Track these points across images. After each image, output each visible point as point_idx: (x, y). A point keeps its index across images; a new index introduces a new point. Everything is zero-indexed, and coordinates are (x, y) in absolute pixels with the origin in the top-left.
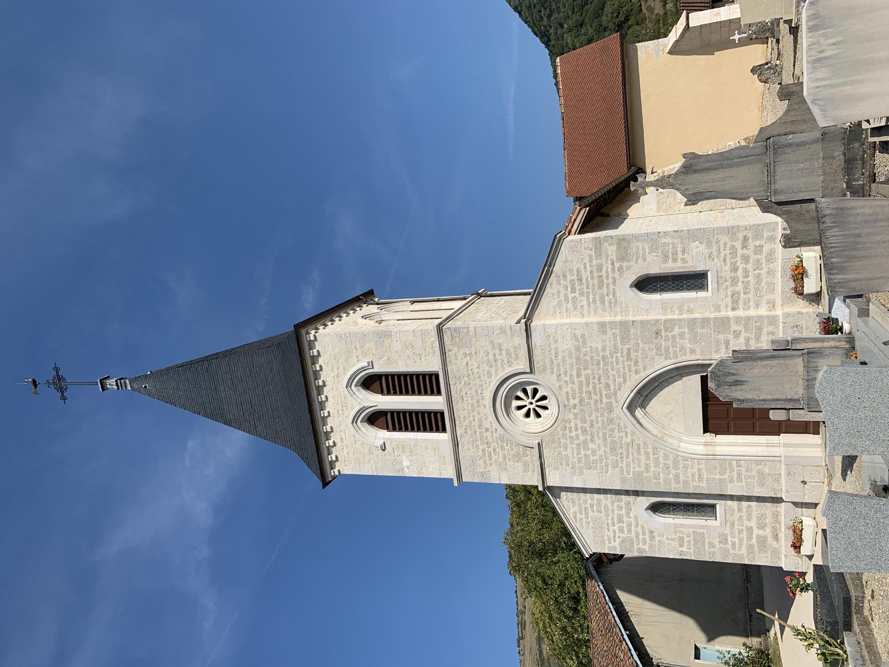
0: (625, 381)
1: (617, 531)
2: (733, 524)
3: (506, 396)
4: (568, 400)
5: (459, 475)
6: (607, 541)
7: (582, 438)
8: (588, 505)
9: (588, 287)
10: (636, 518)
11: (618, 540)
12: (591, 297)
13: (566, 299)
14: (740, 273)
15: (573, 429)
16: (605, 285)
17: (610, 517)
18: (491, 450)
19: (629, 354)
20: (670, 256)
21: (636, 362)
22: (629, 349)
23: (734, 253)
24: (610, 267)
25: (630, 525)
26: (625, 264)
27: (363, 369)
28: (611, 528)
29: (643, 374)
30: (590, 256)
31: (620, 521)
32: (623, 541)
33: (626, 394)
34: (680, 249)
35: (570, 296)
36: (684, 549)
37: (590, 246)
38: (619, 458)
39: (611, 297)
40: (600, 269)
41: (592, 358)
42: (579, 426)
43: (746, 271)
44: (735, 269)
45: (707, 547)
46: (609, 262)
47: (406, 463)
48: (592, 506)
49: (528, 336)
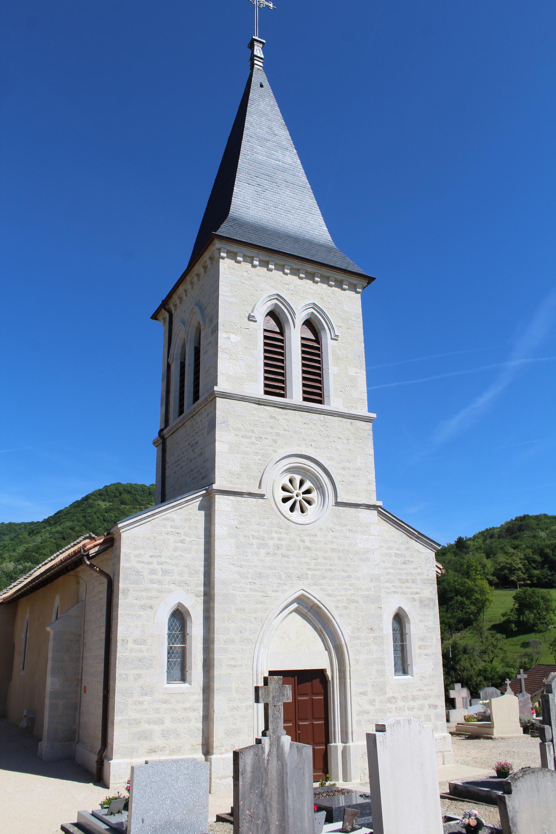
0: (329, 595)
1: (151, 567)
2: (166, 702)
3: (308, 471)
4: (309, 535)
5: (225, 396)
6: (137, 552)
7: (271, 543)
8: (184, 537)
9: (400, 569)
10: (170, 591)
11: (139, 566)
12: (392, 571)
13: (390, 548)
14: (411, 703)
15: (280, 536)
16: (400, 585)
17: (169, 561)
18: (253, 440)
19: (354, 601)
20: (424, 643)
21: (346, 608)
22: (357, 602)
23: (425, 698)
24: (415, 591)
25: (160, 582)
26: (417, 604)
27: (331, 328)
28: (155, 560)
29: (335, 614)
30: (422, 574)
31: (165, 572)
32: (138, 572)
33: (318, 595)
34: (429, 651)
35: (393, 552)
36: (131, 645)
37: (430, 575)
38: (251, 581)
39: (393, 589)
40: (414, 581)
41: (348, 565)
42: (282, 542)
43: (411, 709)
44: (414, 699)
45: (136, 672)
46: (418, 591)
47: (234, 338)
48: (182, 541)
49: (369, 507)
